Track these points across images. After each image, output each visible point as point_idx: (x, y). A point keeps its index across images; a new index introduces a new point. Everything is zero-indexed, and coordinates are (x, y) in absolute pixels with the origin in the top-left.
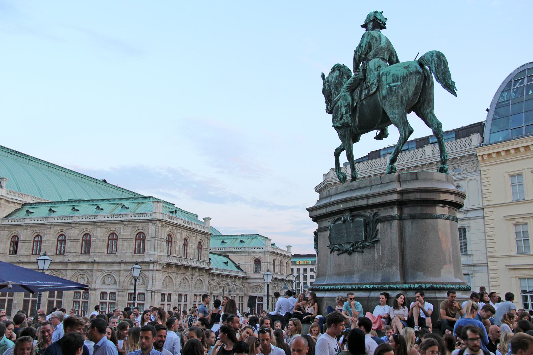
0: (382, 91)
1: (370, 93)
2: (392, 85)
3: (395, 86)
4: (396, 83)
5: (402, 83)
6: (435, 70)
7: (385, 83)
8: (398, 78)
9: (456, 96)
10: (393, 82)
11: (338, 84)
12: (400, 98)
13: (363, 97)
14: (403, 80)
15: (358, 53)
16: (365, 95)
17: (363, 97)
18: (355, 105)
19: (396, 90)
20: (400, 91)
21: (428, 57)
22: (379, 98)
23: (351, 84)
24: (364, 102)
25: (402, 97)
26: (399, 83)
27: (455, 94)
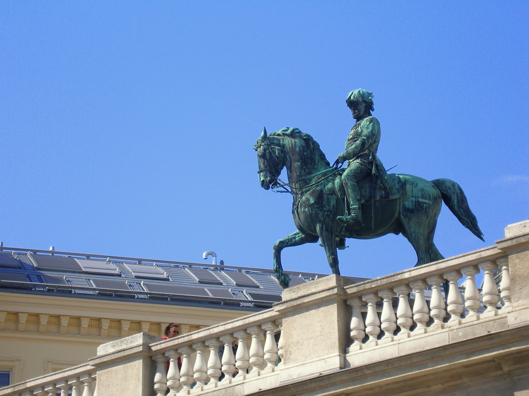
0: (403, 201)
1: (390, 197)
2: (421, 200)
3: (426, 203)
4: (427, 201)
5: (433, 204)
6: (457, 203)
7: (409, 194)
8: (429, 196)
9: (484, 241)
10: (422, 197)
11: (308, 158)
12: (429, 219)
13: (378, 198)
14: (434, 201)
15: (370, 140)
16: (381, 197)
17: (378, 198)
18: (363, 202)
19: (426, 208)
20: (431, 211)
21: (448, 184)
22: (398, 207)
23: (357, 173)
24: (378, 204)
25: (431, 219)
26: (430, 202)
27: (481, 238)
